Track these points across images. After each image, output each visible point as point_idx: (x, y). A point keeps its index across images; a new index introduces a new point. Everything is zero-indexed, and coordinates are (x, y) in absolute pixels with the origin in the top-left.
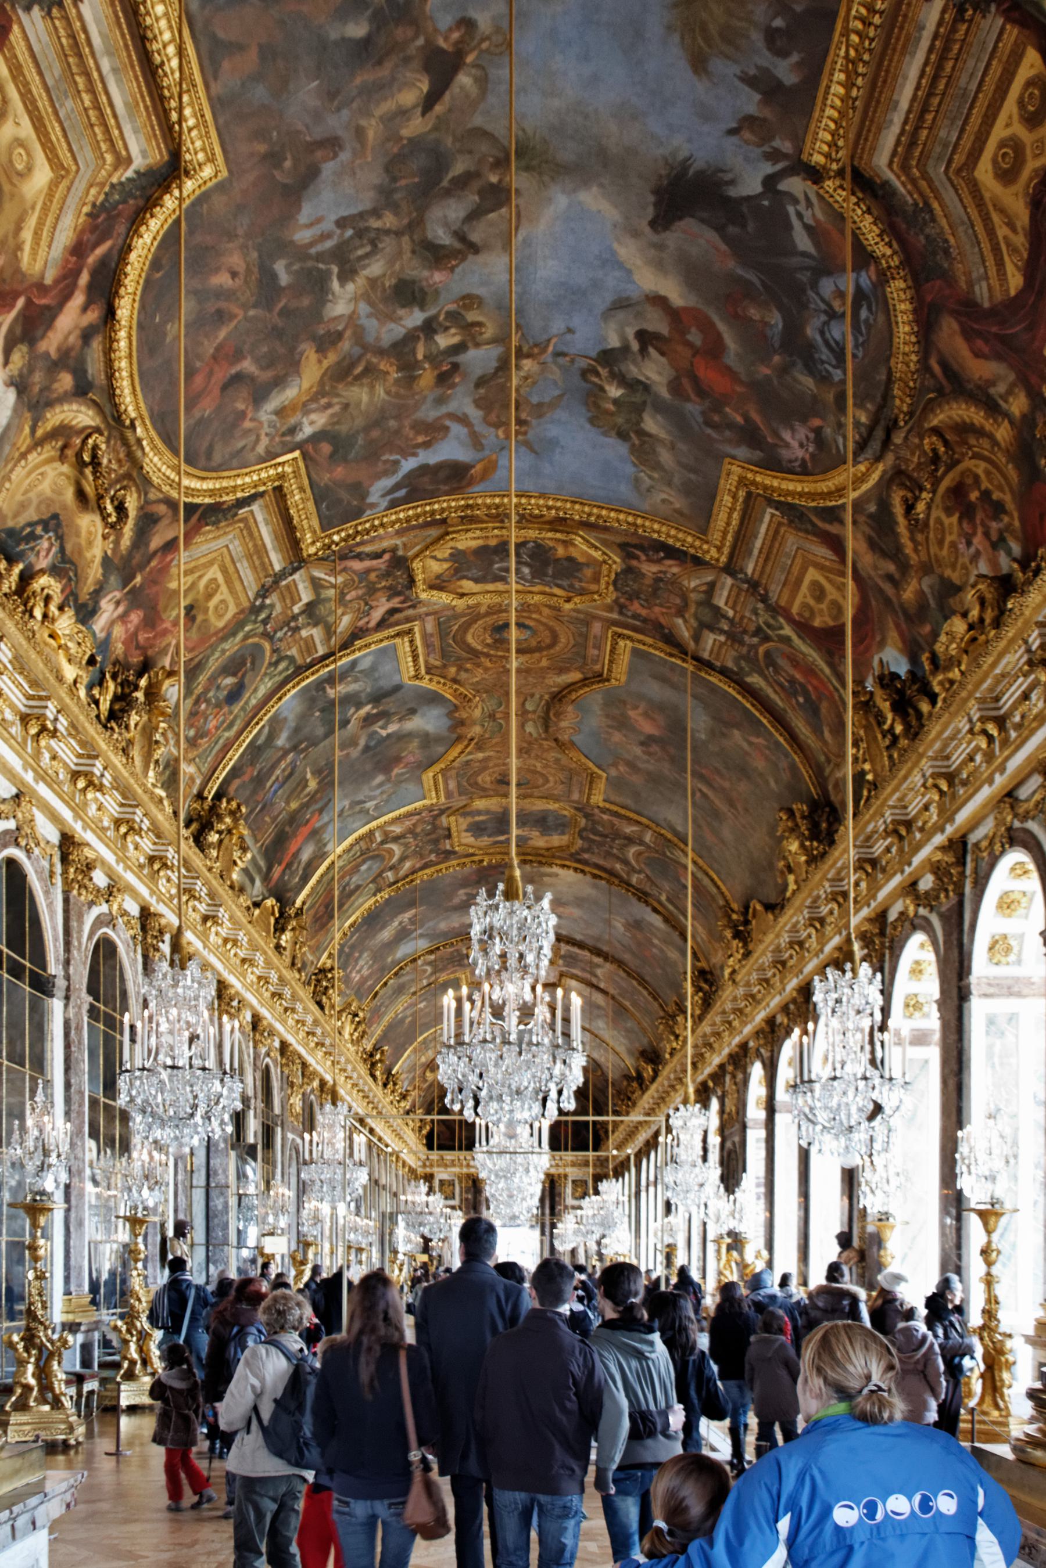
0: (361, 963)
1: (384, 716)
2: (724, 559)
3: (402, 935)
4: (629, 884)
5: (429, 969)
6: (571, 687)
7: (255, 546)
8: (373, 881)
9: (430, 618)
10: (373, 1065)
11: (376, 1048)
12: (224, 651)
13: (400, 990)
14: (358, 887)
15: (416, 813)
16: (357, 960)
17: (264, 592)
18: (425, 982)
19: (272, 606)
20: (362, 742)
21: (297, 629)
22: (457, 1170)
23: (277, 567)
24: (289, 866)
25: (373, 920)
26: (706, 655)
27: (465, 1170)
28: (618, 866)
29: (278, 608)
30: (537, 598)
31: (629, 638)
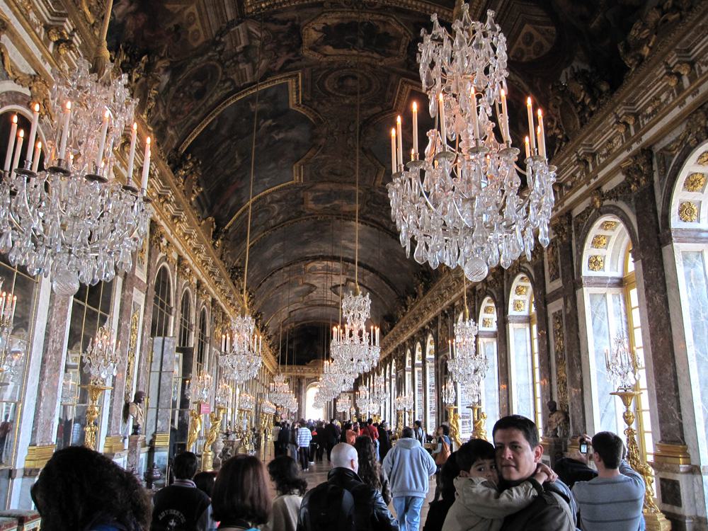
0: (255, 267)
1: (278, 127)
4: (388, 230)
6: (375, 116)
9: (308, 69)
12: (195, 64)
15: (288, 187)
17: (221, 33)
19: (225, 44)
20: (265, 141)
21: (237, 63)
23: (230, 19)
24: (222, 207)
27: (295, 374)
28: (384, 220)
29: (228, 47)
30: (365, 59)
31: (412, 84)
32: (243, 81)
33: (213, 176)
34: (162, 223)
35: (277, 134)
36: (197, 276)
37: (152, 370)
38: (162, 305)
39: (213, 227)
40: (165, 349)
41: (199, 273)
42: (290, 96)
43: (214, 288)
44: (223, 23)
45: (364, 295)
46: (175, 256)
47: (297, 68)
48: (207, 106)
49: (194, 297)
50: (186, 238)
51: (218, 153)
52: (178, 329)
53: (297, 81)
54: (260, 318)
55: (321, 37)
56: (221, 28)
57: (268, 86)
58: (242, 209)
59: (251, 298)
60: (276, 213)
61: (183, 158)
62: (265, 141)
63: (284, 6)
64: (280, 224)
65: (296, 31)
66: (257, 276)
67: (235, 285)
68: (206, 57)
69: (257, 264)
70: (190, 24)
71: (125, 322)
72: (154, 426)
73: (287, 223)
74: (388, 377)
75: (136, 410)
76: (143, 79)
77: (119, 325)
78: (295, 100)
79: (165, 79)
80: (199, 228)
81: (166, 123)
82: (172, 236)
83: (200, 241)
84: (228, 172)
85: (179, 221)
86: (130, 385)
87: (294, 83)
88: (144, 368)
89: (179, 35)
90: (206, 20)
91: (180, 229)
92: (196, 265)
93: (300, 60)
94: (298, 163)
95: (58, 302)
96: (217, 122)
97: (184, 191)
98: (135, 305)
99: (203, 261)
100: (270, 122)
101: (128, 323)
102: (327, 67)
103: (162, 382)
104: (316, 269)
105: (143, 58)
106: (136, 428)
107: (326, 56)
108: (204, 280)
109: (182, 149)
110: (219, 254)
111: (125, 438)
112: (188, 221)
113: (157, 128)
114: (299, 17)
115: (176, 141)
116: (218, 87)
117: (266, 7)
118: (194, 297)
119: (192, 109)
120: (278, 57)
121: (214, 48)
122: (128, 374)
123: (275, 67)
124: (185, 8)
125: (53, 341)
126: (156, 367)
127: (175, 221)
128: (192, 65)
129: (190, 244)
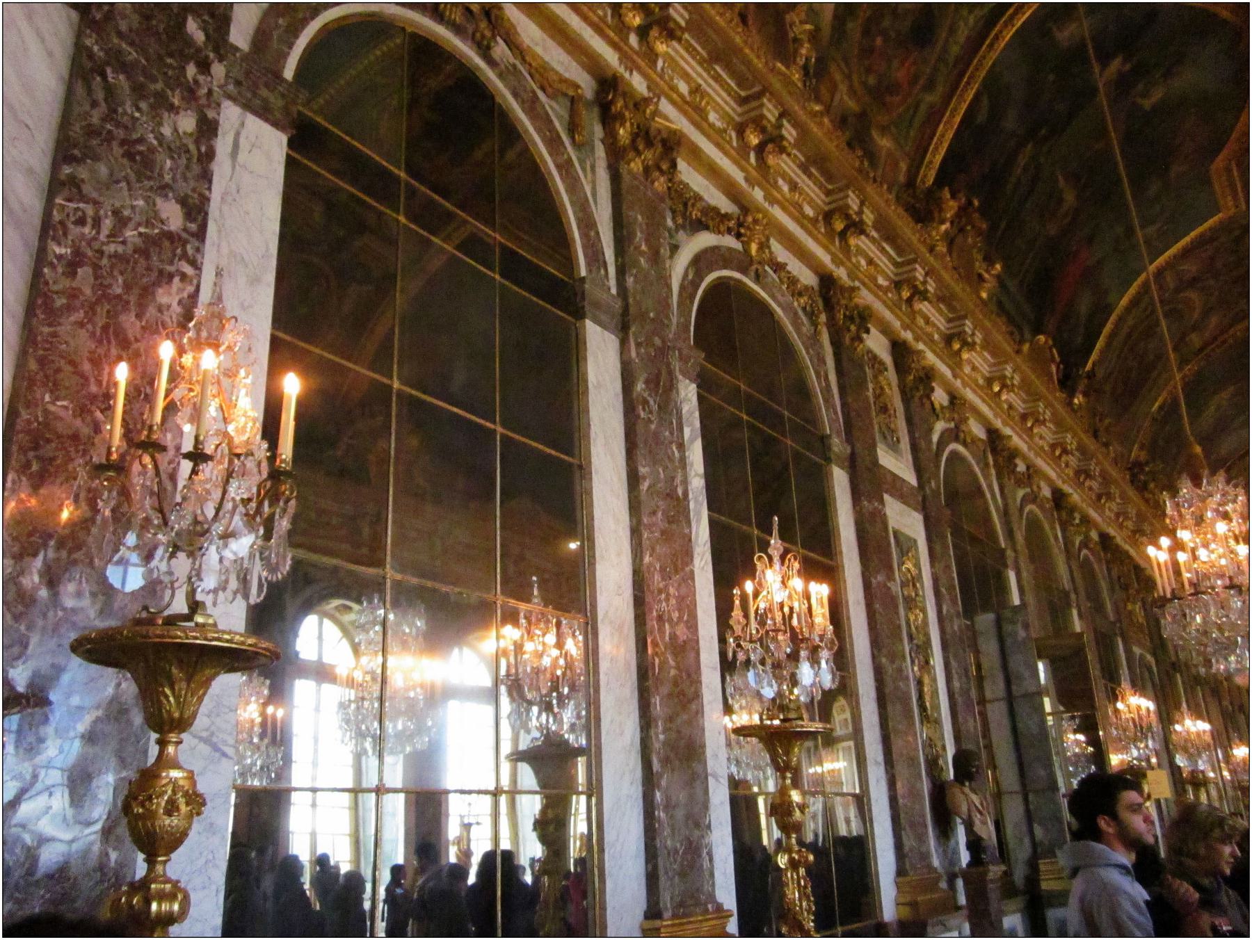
39: (1053, 360)
40: (1009, 642)
48: (951, 60)
49: (1053, 528)
51: (1013, 179)
58: (1113, 318)
60: (1196, 315)
64: (1215, 338)
71: (880, 578)
72: (1027, 841)
73: (1231, 332)
75: (967, 799)
77: (867, 586)
81: (862, 116)
82: (958, 383)
83: (1032, 395)
84: (1053, 229)
85: (965, 343)
86: (935, 737)
88: (965, 692)
91: (974, 368)
92: (1037, 454)
94: (1221, 157)
95: (654, 513)
96: (985, 101)
98: (902, 539)
101: (890, 577)
103: (1020, 725)
106: (975, 845)
111: (952, 878)
115: (903, 166)
118: (1053, 528)
122: (922, 707)
125: (660, 618)
126: (996, 688)
127: (956, 346)
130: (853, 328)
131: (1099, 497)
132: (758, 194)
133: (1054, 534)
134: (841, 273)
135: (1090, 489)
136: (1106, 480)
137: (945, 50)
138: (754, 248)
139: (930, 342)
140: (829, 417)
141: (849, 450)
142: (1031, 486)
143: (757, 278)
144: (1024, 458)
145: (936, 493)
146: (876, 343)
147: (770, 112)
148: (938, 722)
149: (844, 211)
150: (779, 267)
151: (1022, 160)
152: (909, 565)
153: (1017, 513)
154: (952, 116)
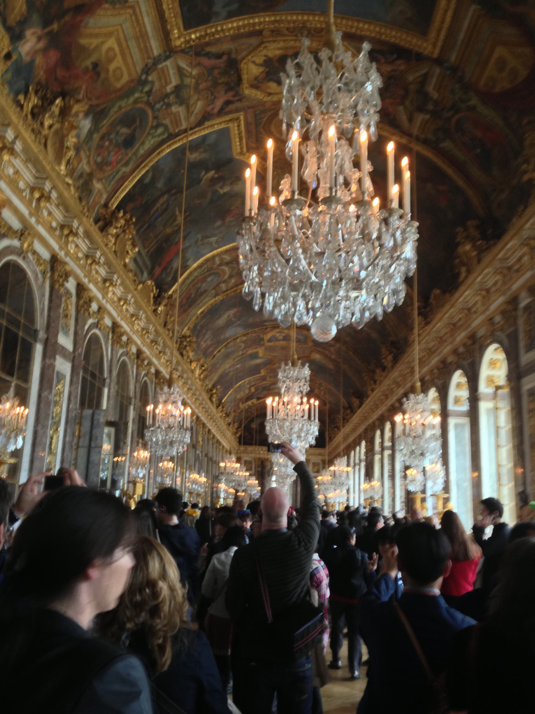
0: (207, 336)
2: (437, 51)
3: (229, 324)
5: (243, 345)
7: (141, 31)
8: (214, 289)
10: (212, 395)
11: (214, 386)
13: (227, 356)
14: (205, 291)
16: (204, 335)
17: (147, 70)
18: (241, 353)
19: (152, 83)
20: (209, 196)
21: (169, 105)
22: (253, 455)
23: (156, 52)
25: (213, 312)
26: (415, 131)
27: (258, 456)
29: (157, 86)
32: (177, 126)
33: (151, 235)
34: (91, 286)
35: (221, 188)
36: (137, 345)
37: (81, 444)
38: (93, 375)
39: (153, 291)
40: (95, 422)
41: (139, 342)
42: (233, 144)
43: (159, 359)
44: (149, 58)
45: (303, 365)
46: (108, 322)
47: (237, 111)
48: (138, 156)
50: (122, 303)
51: (155, 208)
52: (112, 402)
53: (239, 126)
54: (215, 393)
55: (262, 72)
56: (146, 65)
57: (207, 132)
59: (204, 370)
60: (226, 277)
61: (114, 214)
62: (209, 196)
63: (217, 36)
65: (233, 65)
66: (209, 347)
67: (182, 355)
68: (132, 99)
69: (209, 333)
70: (110, 60)
74: (357, 461)
76: (57, 126)
77: (40, 396)
78: (238, 147)
79: (86, 124)
80: (135, 292)
81: (91, 175)
83: (138, 307)
84: (169, 230)
87: (236, 128)
88: (71, 442)
89: (98, 74)
90: (128, 56)
91: (114, 293)
93: (240, 100)
96: (150, 174)
97: (115, 252)
99: (143, 329)
100: (211, 173)
102: (273, 107)
104: (277, 340)
105: (58, 101)
107: (270, 94)
108: (145, 349)
109: (112, 205)
110: (162, 320)
112: (122, 284)
113: (81, 181)
114: (236, 50)
115: (105, 196)
116: (149, 134)
117: (197, 38)
118: (132, 367)
119: (121, 160)
120: (215, 98)
121: (140, 88)
123: (213, 109)
124: (103, 43)
126: (84, 442)
127: (107, 284)
128: (116, 109)
129: (127, 310)
130: (61, 280)
131: (160, 352)
132: (33, 220)
133: (132, 370)
134: (62, 254)
135: (157, 348)
136: (165, 345)
137: (138, 150)
138: (26, 245)
139: (96, 284)
140: (40, 322)
141: (46, 336)
142: (127, 347)
143: (24, 258)
144: (128, 335)
145: (80, 355)
146: (71, 285)
147: (48, 186)
148: (55, 455)
149: (70, 227)
150: (34, 253)
151: (161, 201)
152: (59, 387)
153: (116, 362)
154: (131, 181)
